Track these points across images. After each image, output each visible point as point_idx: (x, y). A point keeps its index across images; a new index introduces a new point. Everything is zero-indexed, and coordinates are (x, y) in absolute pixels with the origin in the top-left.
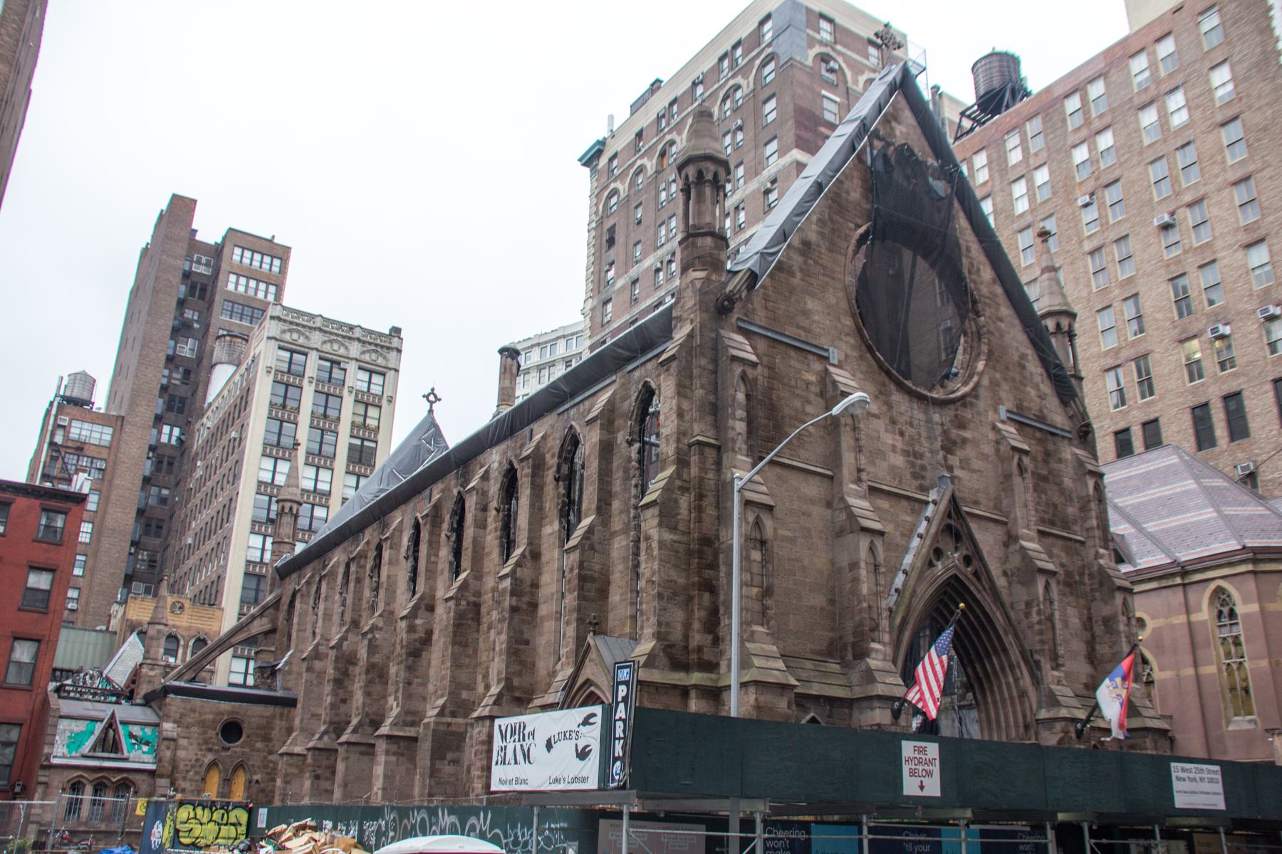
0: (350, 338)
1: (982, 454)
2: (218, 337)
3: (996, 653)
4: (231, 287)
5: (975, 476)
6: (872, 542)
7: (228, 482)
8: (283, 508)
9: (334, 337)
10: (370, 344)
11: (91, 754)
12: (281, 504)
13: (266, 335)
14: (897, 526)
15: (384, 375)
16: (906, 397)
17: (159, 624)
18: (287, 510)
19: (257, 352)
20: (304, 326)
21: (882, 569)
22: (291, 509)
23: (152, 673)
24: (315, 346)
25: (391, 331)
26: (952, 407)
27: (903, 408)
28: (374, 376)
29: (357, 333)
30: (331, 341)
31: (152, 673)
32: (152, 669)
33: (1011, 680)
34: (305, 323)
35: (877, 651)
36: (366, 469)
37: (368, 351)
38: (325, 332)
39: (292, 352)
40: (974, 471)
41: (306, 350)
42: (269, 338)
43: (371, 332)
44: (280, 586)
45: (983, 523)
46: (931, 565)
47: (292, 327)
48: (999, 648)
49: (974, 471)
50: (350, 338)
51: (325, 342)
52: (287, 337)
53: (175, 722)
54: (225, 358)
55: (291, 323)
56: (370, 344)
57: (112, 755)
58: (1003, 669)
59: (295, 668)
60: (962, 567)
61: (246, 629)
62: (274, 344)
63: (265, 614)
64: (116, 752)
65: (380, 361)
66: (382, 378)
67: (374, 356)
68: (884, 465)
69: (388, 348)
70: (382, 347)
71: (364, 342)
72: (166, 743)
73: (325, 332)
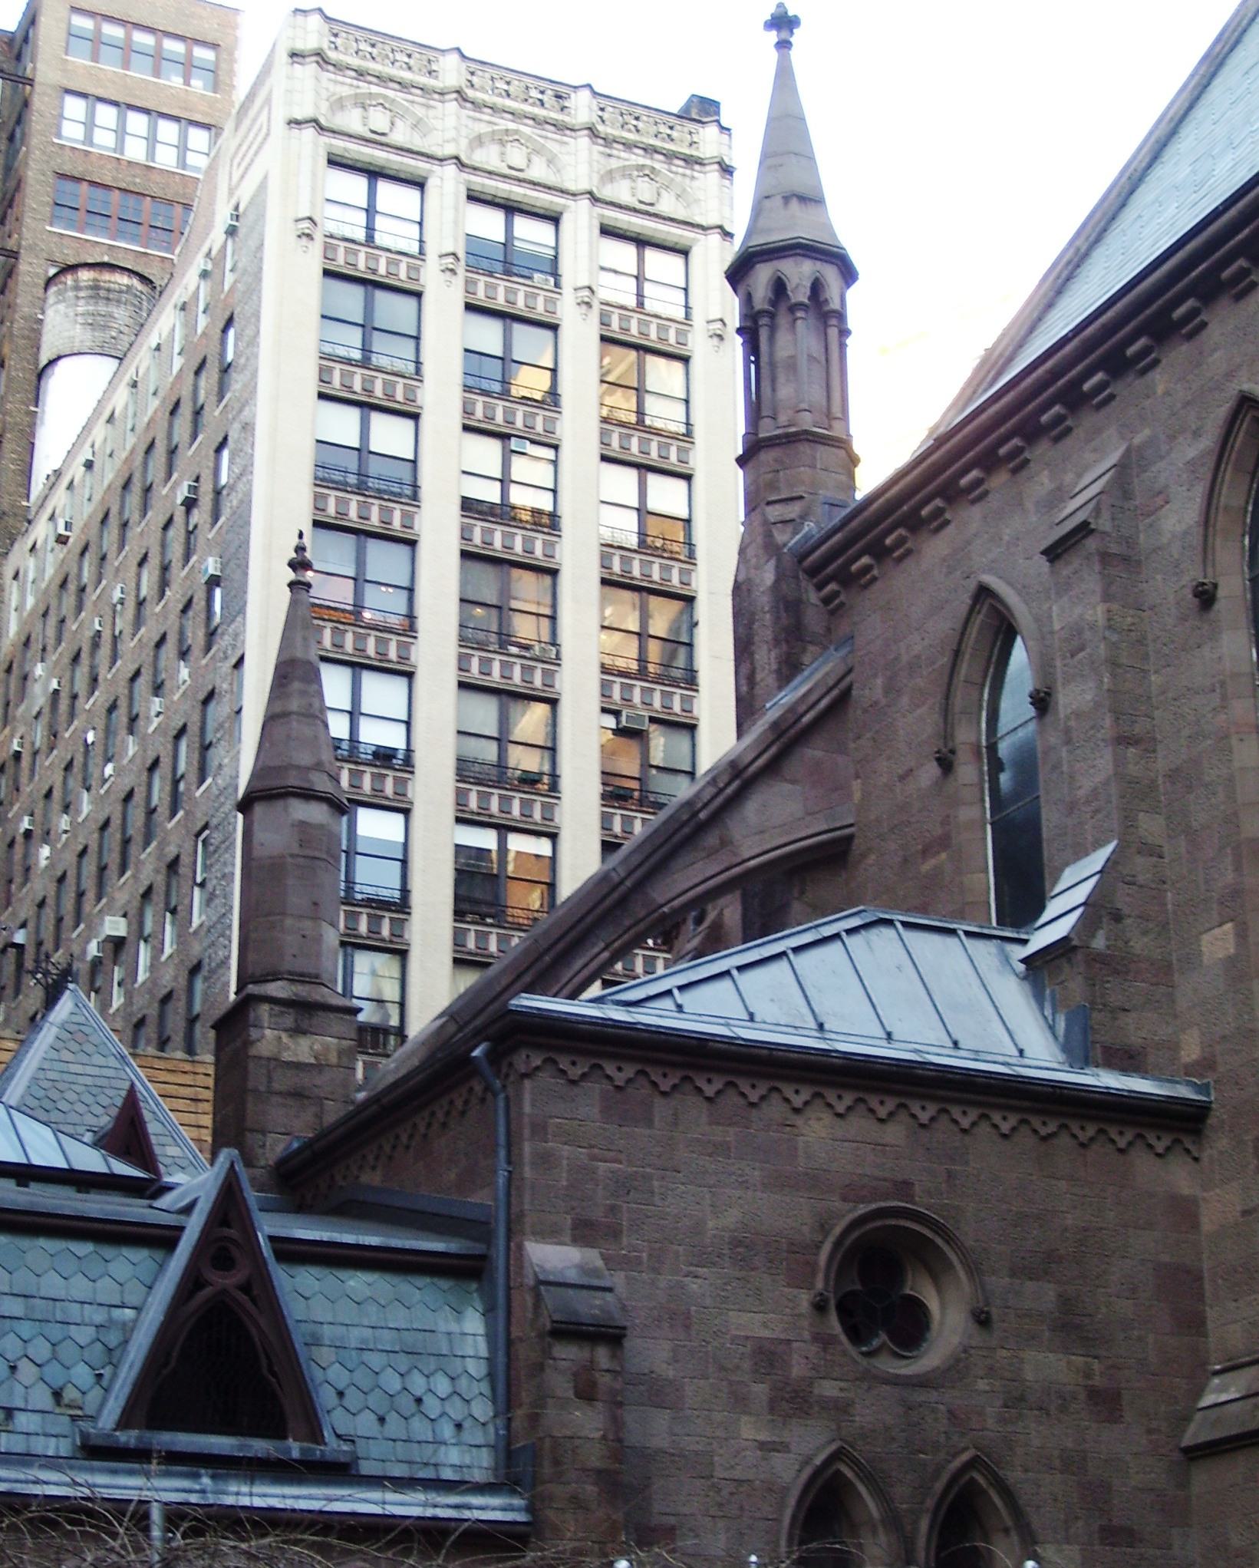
0: (561, 127)
2: (49, 282)
4: (72, 132)
7: (184, 654)
8: (779, 287)
9: (506, 123)
10: (628, 146)
11: (129, 1438)
12: (762, 276)
13: (280, 116)
15: (685, 252)
17: (308, 795)
18: (802, 296)
19: (245, 194)
20: (403, 85)
22: (817, 287)
23: (302, 1049)
24: (449, 150)
25: (687, 108)
28: (650, 254)
29: (582, 110)
30: (502, 139)
31: (302, 1049)
32: (297, 1031)
34: (407, 76)
36: (666, 569)
37: (625, 172)
38: (477, 105)
39: (374, 174)
41: (419, 166)
42: (295, 123)
43: (631, 111)
44: (826, 640)
47: (364, 88)
50: (561, 127)
51: (478, 141)
52: (352, 120)
53: (584, 1232)
54: (81, 336)
55: (361, 74)
56: (628, 146)
57: (260, 1447)
59: (1140, 944)
61: (711, 839)
62: (311, 146)
63: (795, 766)
64: (277, 1431)
65: (667, 205)
66: (677, 261)
67: (645, 190)
69: (691, 161)
70: (670, 156)
71: (608, 141)
72: (568, 1353)
73: (477, 105)
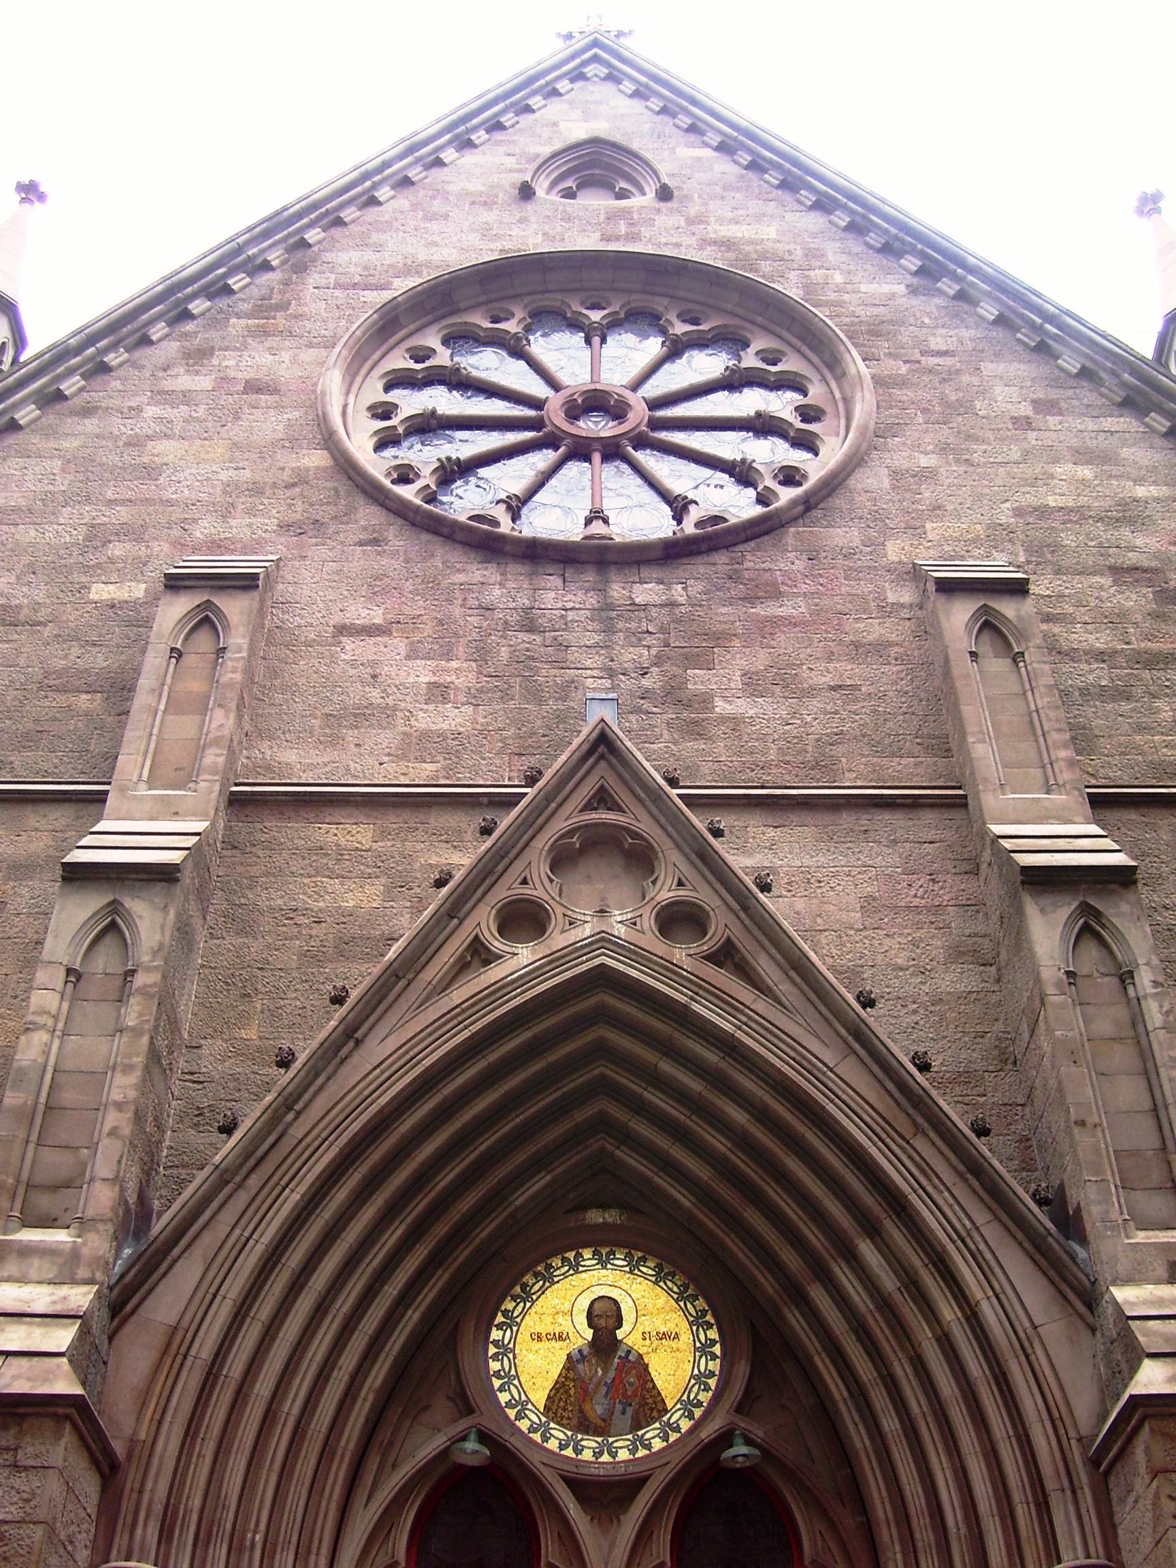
1: (857, 645)
3: (873, 1231)
5: (815, 704)
6: (114, 907)
14: (399, 885)
16: (516, 569)
21: (140, 980)
26: (721, 558)
27: (495, 594)
33: (949, 1312)
35: (26, 1251)
40: (812, 692)
45: (846, 819)
46: (479, 954)
48: (868, 1199)
49: (812, 692)
58: (912, 1285)
60: (651, 941)
68: (386, 739)
